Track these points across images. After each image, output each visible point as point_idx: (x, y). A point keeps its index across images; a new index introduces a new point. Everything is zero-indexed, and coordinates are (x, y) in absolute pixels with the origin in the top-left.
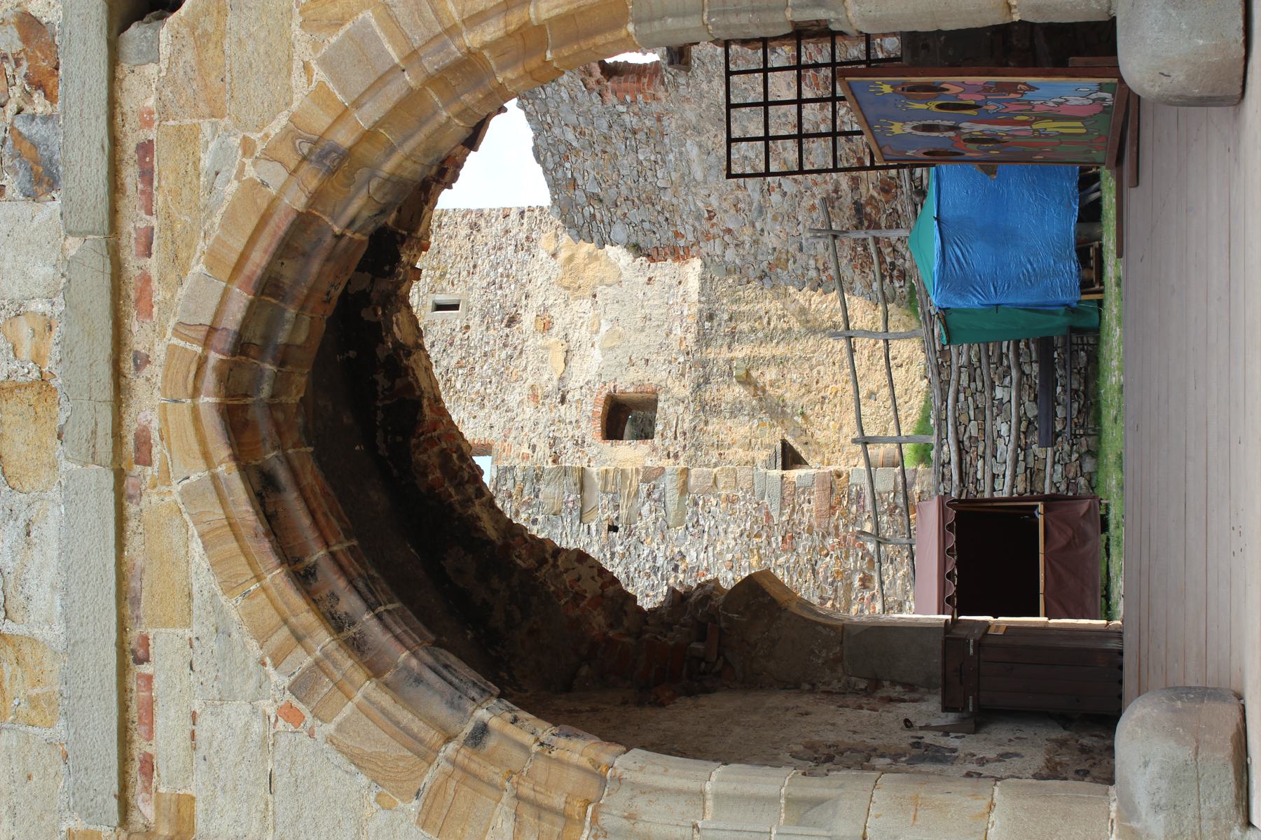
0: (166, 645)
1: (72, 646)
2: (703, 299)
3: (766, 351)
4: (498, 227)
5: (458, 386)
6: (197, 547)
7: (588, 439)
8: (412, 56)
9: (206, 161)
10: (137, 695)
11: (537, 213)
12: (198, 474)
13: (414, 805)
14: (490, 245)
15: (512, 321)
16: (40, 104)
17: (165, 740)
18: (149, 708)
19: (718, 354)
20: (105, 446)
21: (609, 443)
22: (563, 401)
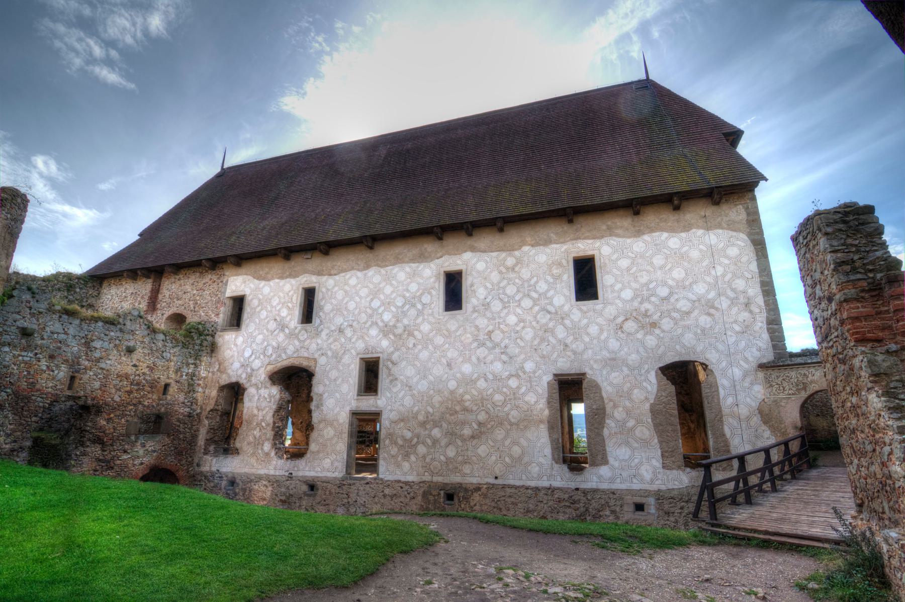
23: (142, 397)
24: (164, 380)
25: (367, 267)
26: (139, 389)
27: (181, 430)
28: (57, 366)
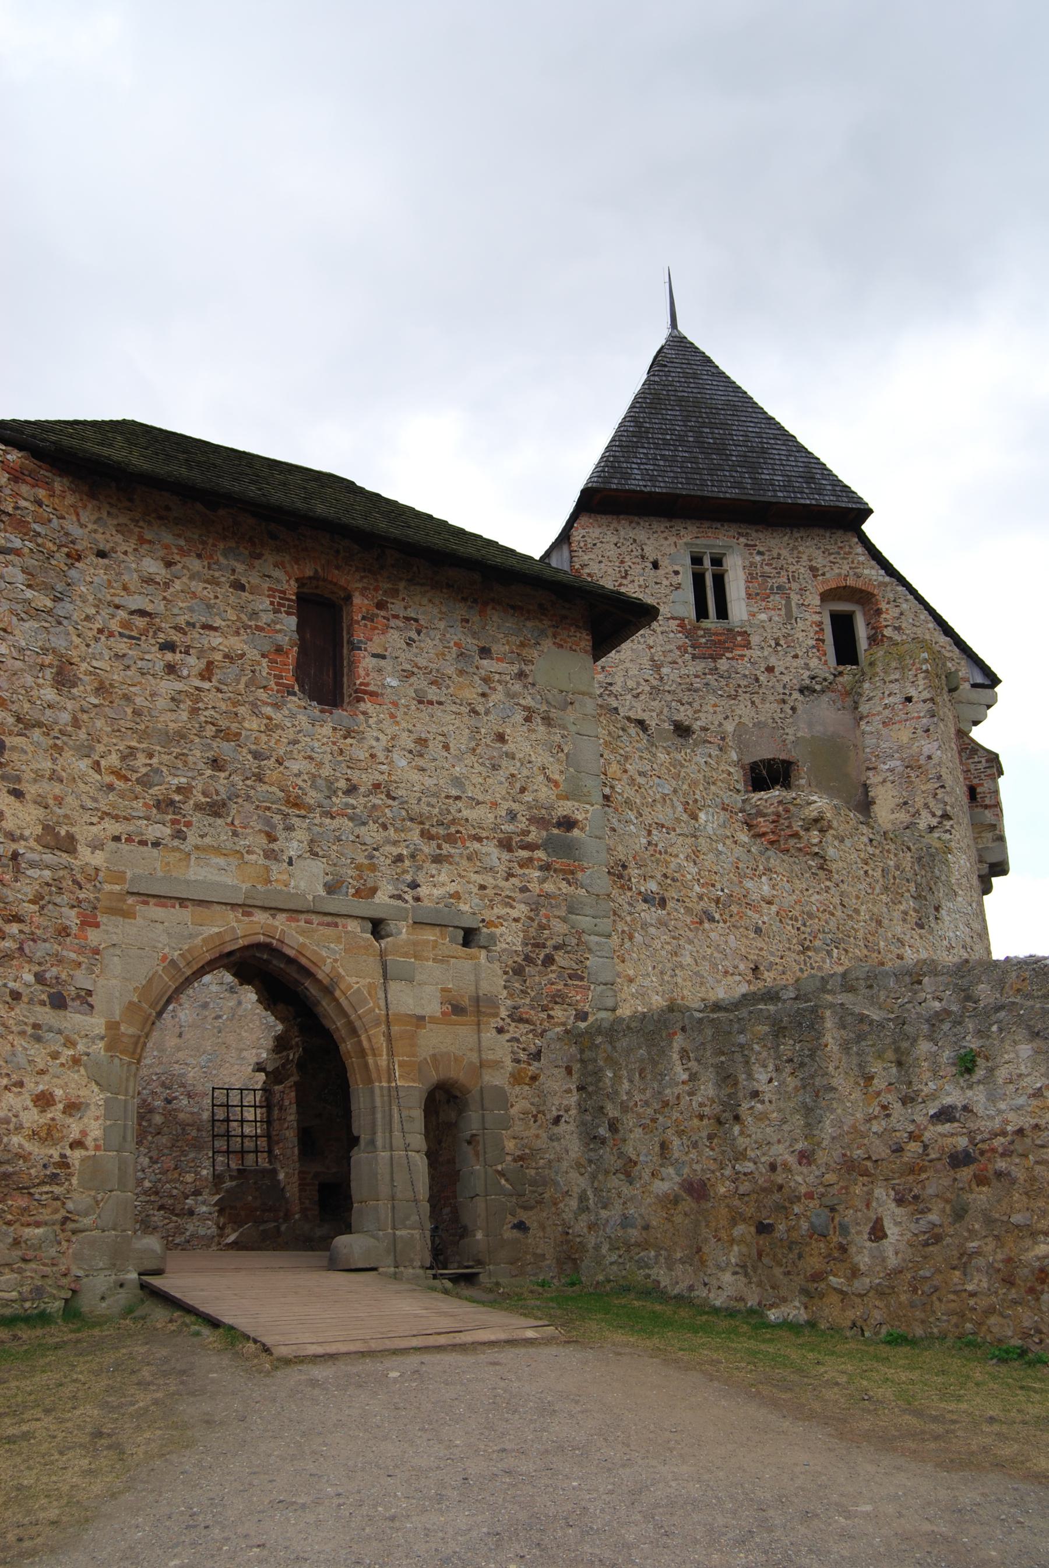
0: (185, 915)
1: (187, 882)
6: (216, 930)
8: (360, 1017)
9: (332, 946)
10: (169, 902)
12: (240, 933)
13: (136, 1000)
16: (352, 891)
17: (155, 911)
18: (164, 906)
20: (250, 902)
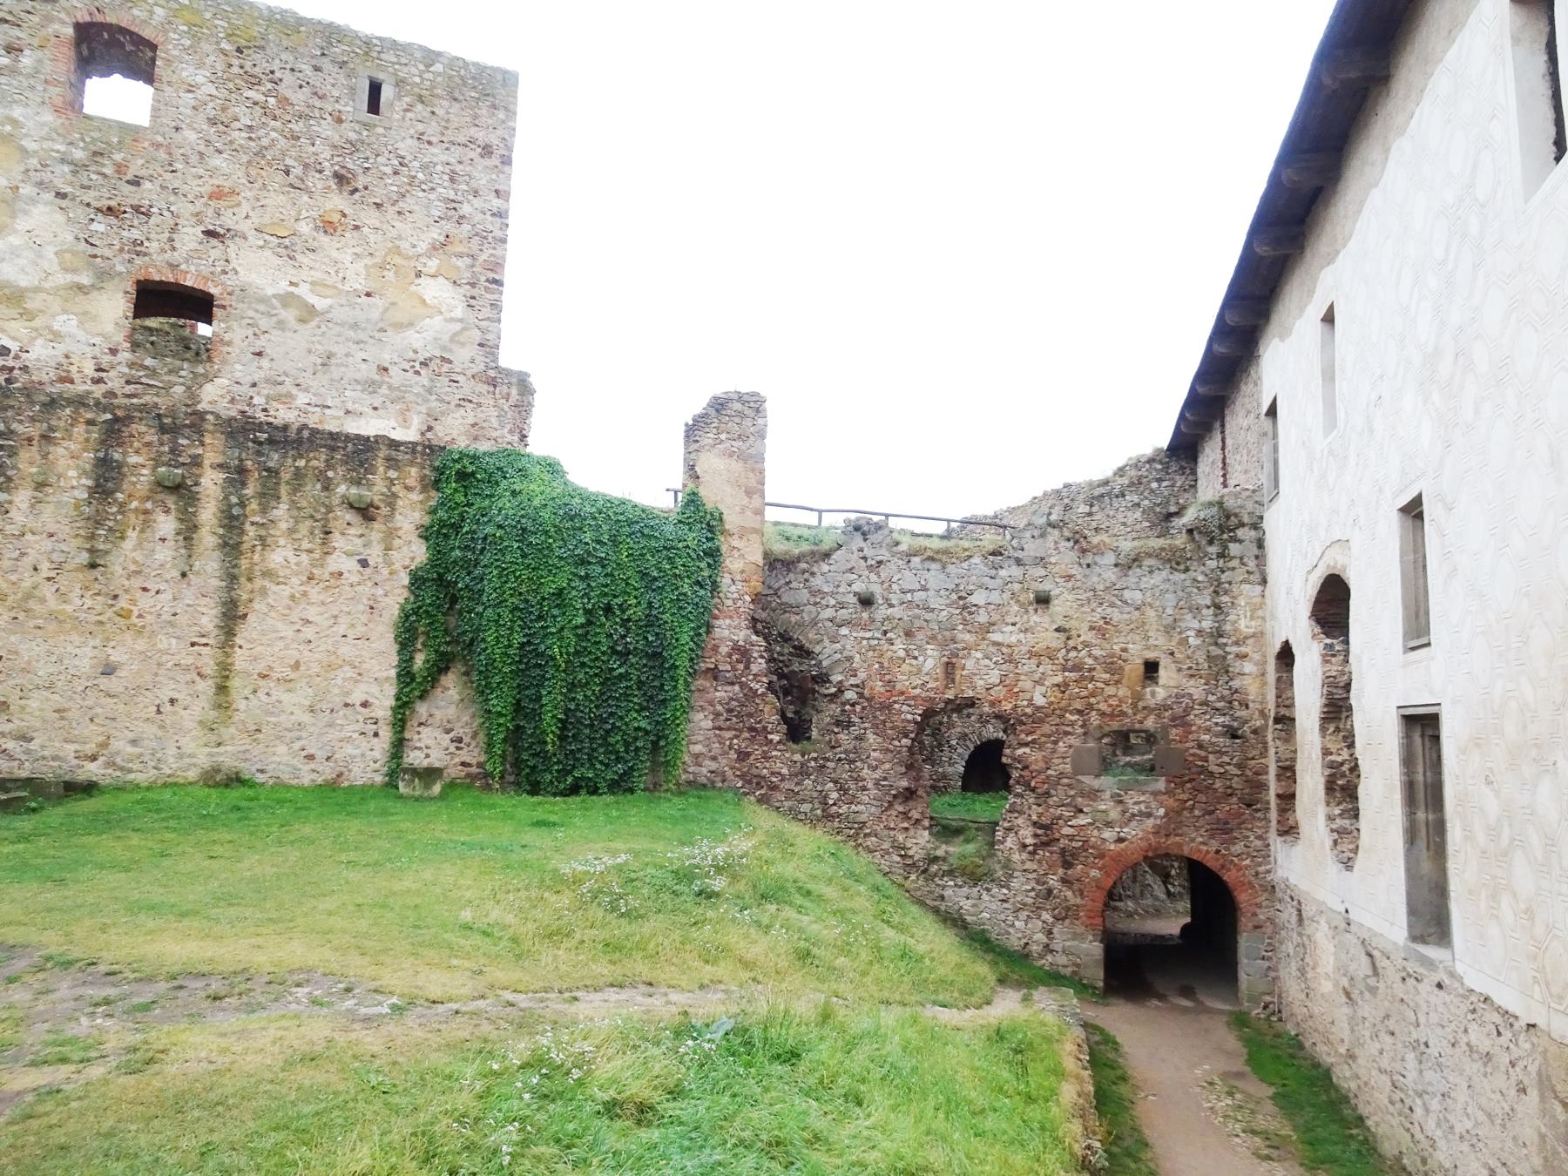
2: (306, 434)
3: (208, 514)
4: (482, 180)
5: (250, 94)
7: (138, 261)
11: (498, 233)
14: (458, 168)
15: (341, 179)
19: (213, 450)
21: (132, 289)
22: (210, 234)
23: (1093, 695)
24: (1138, 652)
25: (1387, 151)
26: (1083, 678)
27: (1214, 768)
28: (919, 648)
